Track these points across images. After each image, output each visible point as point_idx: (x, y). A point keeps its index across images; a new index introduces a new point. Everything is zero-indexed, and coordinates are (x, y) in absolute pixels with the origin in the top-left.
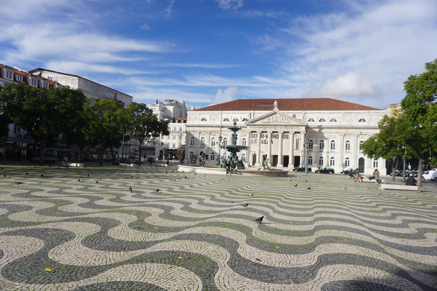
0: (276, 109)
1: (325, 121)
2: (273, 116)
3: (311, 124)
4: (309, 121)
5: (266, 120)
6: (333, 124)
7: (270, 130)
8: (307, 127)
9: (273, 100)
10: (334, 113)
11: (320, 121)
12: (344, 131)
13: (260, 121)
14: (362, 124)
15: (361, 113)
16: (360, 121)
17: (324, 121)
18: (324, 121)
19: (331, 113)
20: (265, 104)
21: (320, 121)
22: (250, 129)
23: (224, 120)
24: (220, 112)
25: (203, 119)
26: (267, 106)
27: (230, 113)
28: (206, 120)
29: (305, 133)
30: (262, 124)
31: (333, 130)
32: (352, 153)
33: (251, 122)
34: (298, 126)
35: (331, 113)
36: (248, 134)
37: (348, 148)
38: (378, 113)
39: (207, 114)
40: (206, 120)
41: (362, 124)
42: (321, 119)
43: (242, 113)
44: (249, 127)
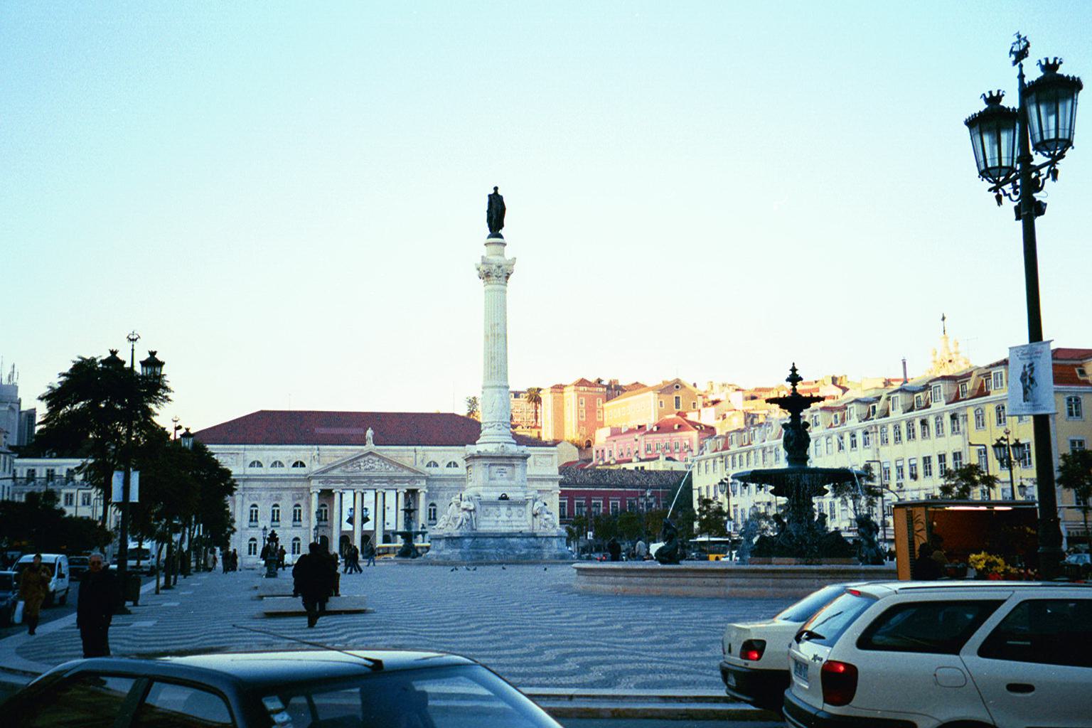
0: (370, 446)
1: (457, 466)
11: (448, 466)
13: (339, 469)
21: (448, 466)
23: (251, 466)
24: (242, 446)
29: (427, 491)
33: (323, 472)
34: (412, 479)
42: (450, 463)
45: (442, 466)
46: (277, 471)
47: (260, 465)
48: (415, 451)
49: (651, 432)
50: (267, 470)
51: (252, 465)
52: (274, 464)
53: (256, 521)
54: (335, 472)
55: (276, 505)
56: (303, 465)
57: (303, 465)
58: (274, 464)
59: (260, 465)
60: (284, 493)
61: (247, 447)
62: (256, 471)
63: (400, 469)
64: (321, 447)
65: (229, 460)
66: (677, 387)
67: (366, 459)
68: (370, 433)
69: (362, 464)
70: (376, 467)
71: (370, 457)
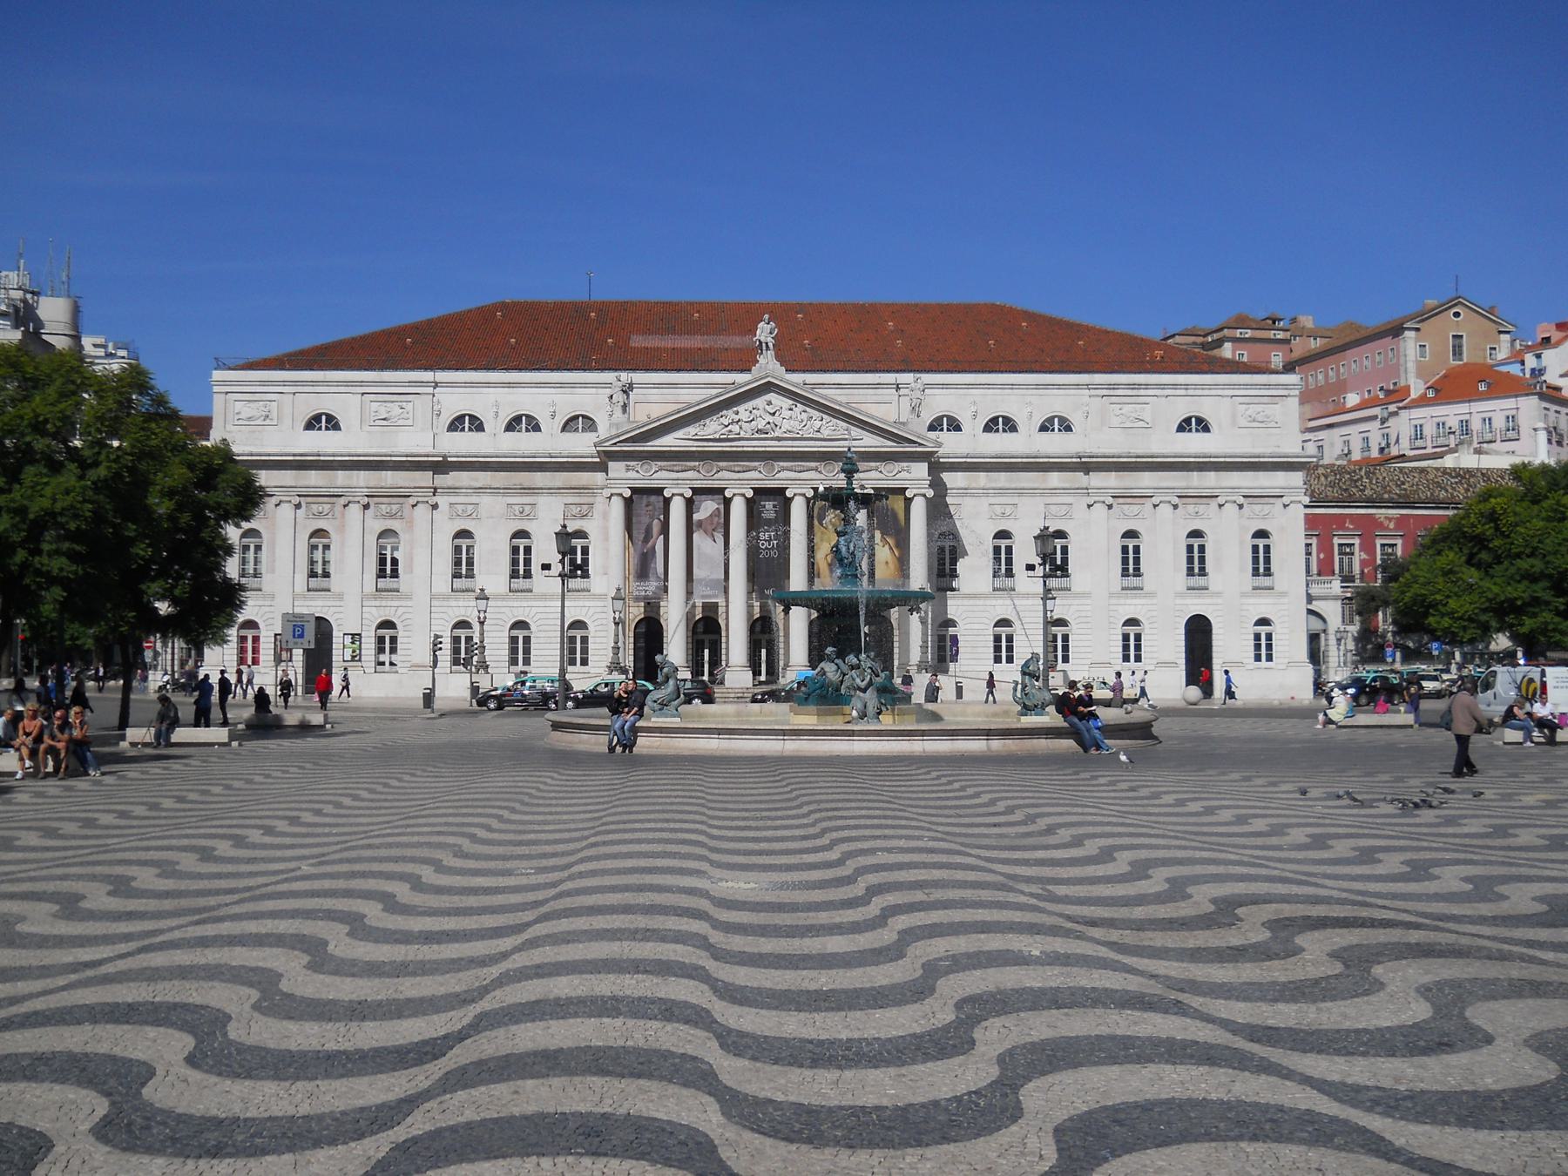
0: (768, 366)
1: (1013, 429)
2: (750, 405)
3: (950, 445)
4: (932, 428)
5: (712, 427)
6: (1055, 445)
7: (739, 484)
8: (937, 467)
9: (746, 317)
10: (1059, 386)
12: (1111, 480)
13: (680, 434)
14: (1194, 444)
15: (1186, 386)
16: (1181, 429)
17: (1010, 425)
18: (1010, 425)
19: (1047, 386)
20: (673, 331)
22: (624, 476)
24: (428, 376)
25: (317, 418)
26: (695, 342)
27: (488, 384)
28: (336, 427)
29: (930, 493)
30: (694, 447)
31: (1055, 479)
32: (1152, 595)
33: (632, 440)
35: (1047, 386)
36: (617, 507)
37: (1131, 567)
38: (1268, 386)
39: (341, 391)
40: (336, 427)
41: (1194, 444)
42: (994, 420)
43: (562, 385)
44: (616, 468)
45: (972, 427)
46: (523, 444)
47: (477, 425)
48: (898, 388)
49: (1422, 402)
50: (494, 442)
51: (456, 424)
52: (513, 425)
53: (470, 575)
54: (668, 442)
55: (521, 534)
56: (590, 424)
57: (590, 424)
58: (513, 425)
59: (477, 425)
60: (543, 501)
61: (442, 376)
62: (464, 444)
63: (856, 432)
64: (638, 377)
65: (396, 410)
66: (1457, 315)
67: (759, 402)
68: (765, 332)
69: (744, 415)
70: (786, 425)
71: (772, 396)
